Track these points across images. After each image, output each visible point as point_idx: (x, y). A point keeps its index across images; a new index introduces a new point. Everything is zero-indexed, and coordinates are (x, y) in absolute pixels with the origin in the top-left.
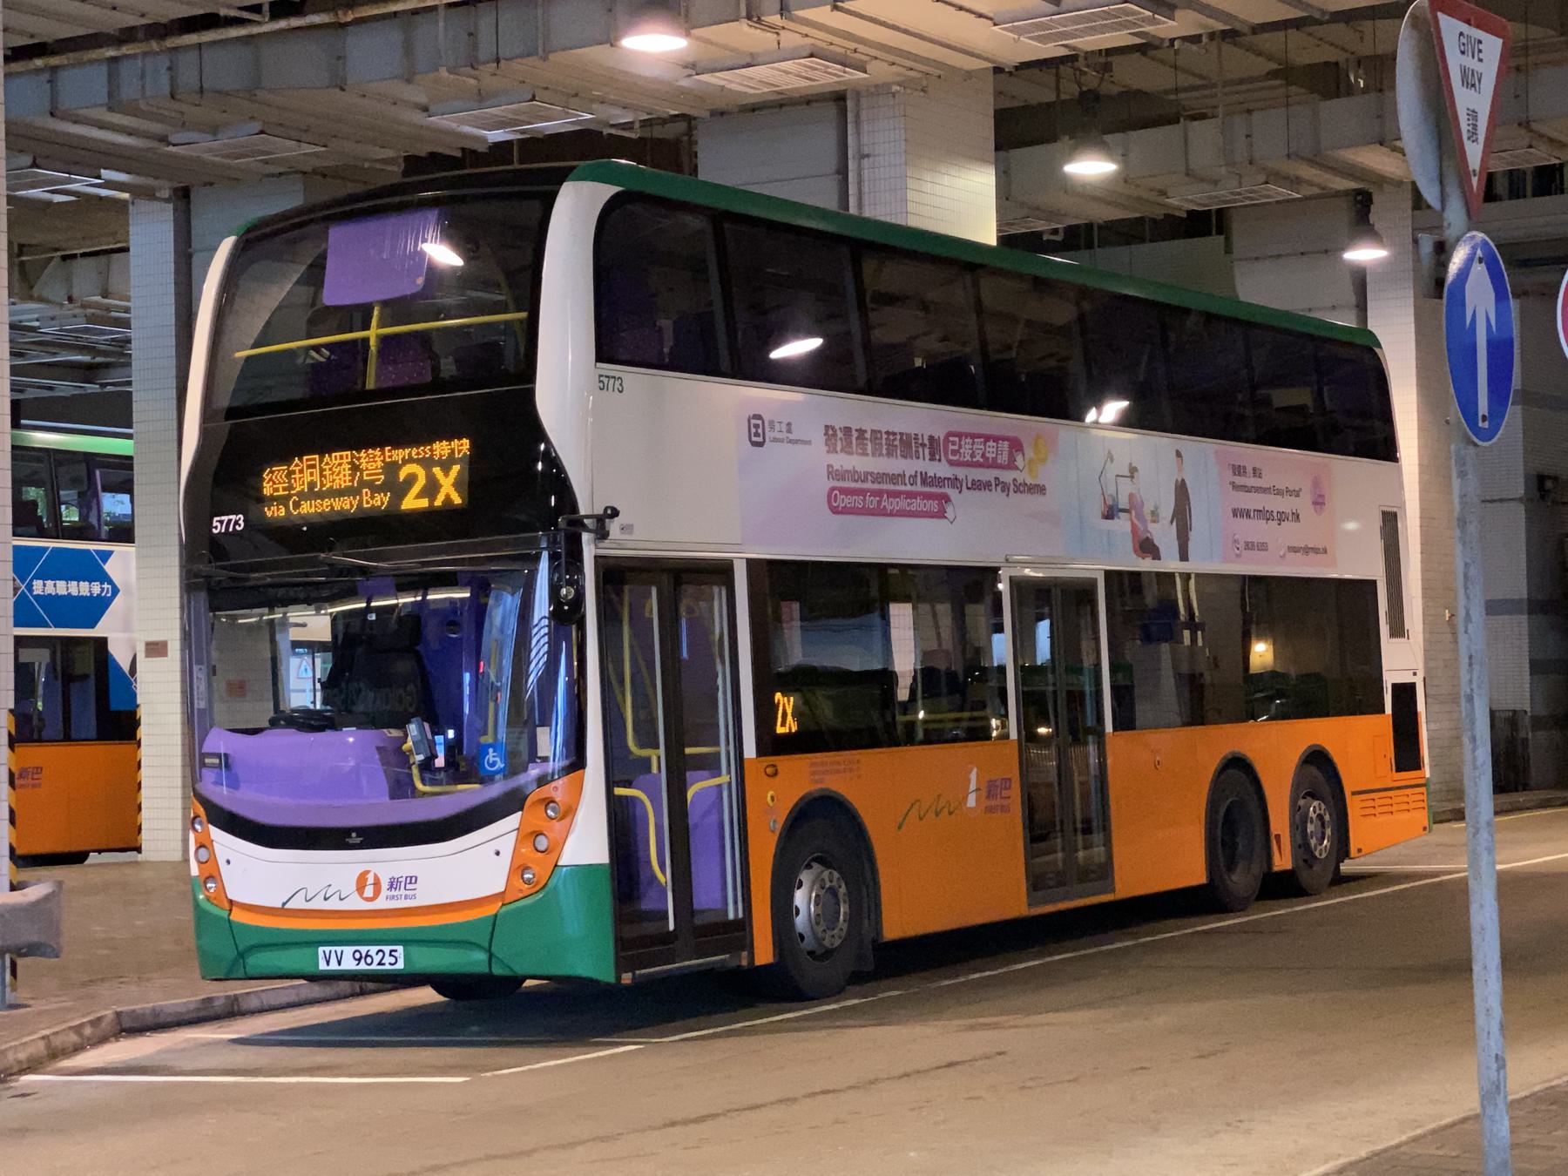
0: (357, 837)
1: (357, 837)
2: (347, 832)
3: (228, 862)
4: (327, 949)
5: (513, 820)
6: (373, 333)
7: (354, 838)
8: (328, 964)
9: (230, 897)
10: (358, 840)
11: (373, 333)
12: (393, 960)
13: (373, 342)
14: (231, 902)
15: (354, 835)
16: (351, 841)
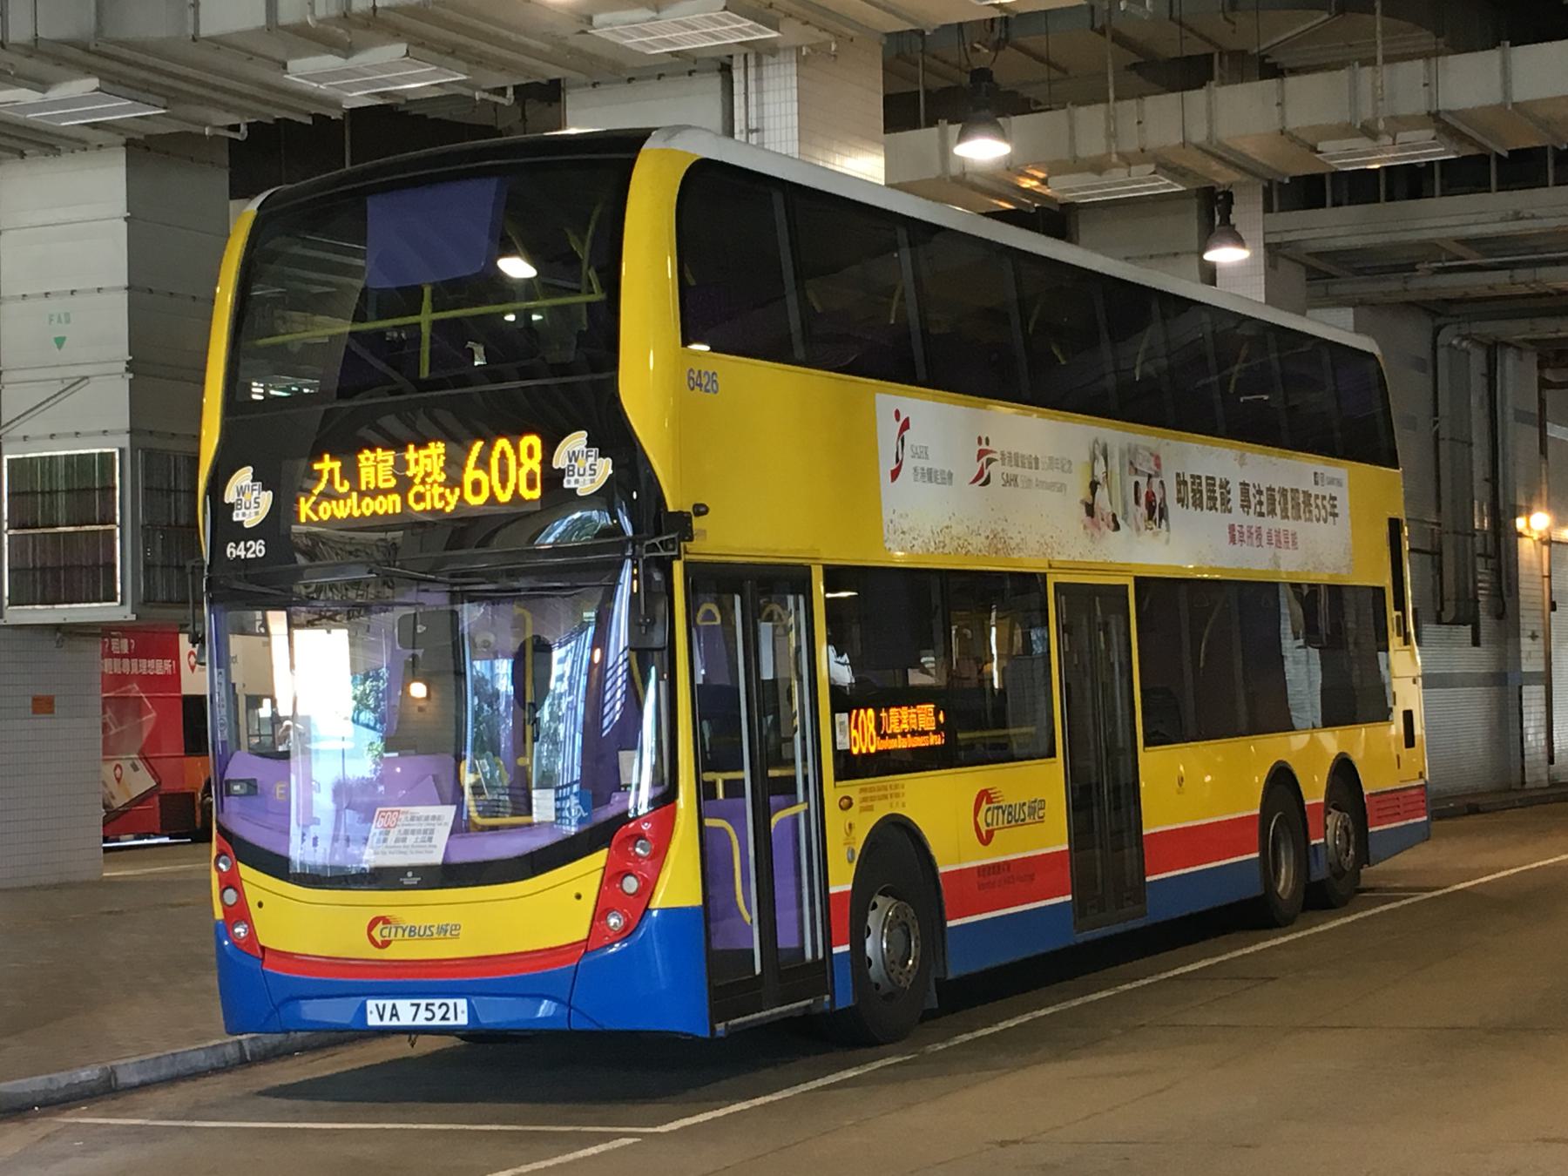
0: (413, 876)
1: (413, 876)
2: (402, 871)
3: (260, 905)
4: (381, 1003)
5: (600, 858)
6: (426, 318)
7: (410, 879)
8: (381, 1017)
9: (262, 944)
10: (415, 881)
11: (426, 318)
12: (429, 1015)
13: (426, 330)
14: (263, 949)
15: (410, 874)
16: (406, 882)
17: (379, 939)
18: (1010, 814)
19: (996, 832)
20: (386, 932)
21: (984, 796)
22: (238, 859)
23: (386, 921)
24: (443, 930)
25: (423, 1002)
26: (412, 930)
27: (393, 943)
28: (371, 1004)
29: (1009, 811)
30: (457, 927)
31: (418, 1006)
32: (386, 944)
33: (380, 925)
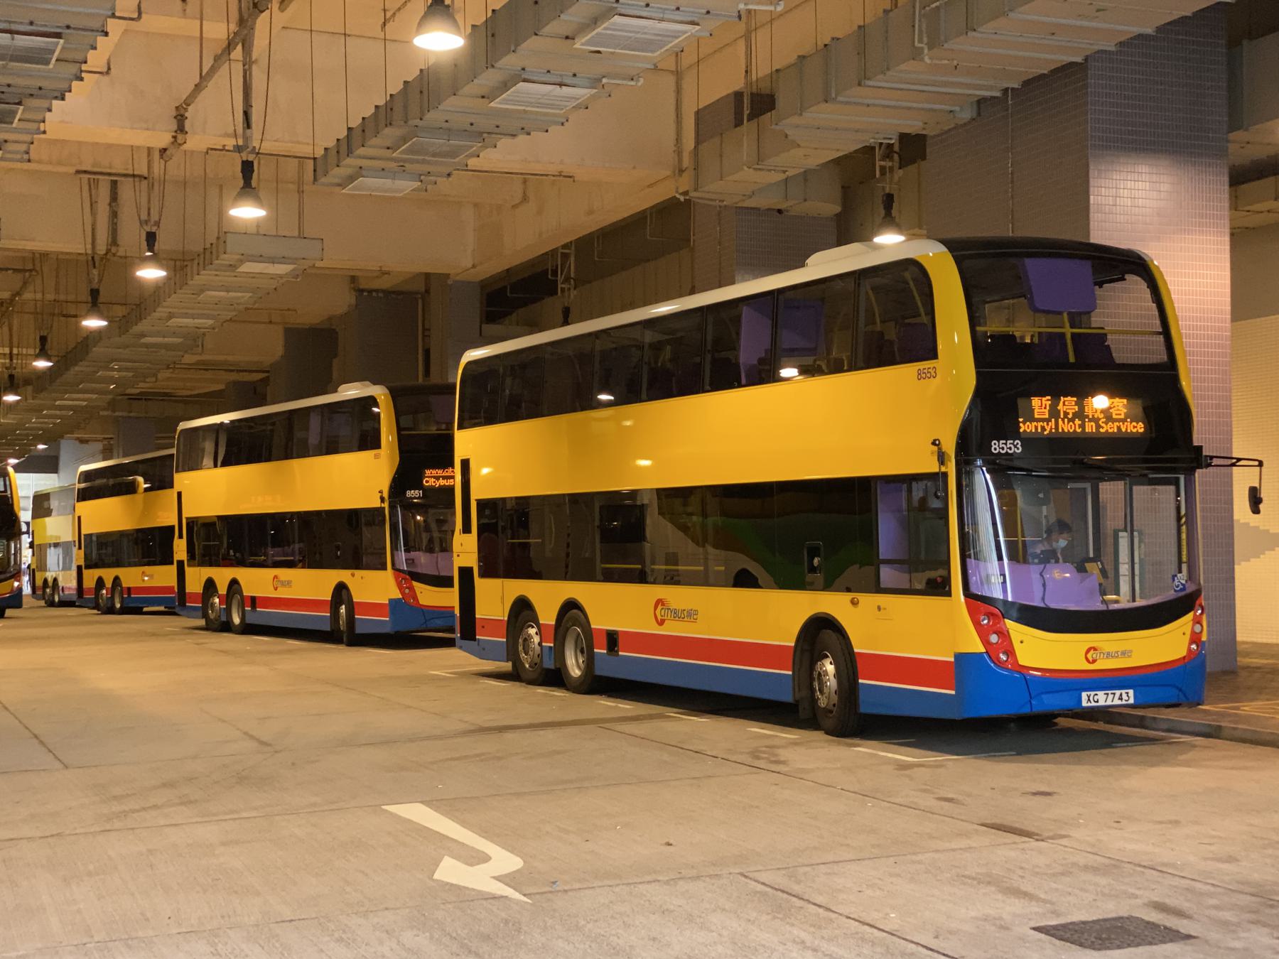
4: (1089, 693)
17: (1091, 659)
18: (675, 613)
19: (666, 622)
20: (1094, 656)
21: (659, 602)
22: (1004, 618)
23: (1095, 649)
24: (1124, 653)
25: (1110, 692)
26: (1108, 653)
27: (1098, 661)
28: (1084, 695)
29: (675, 612)
30: (1131, 651)
31: (1107, 694)
32: (1094, 661)
33: (1092, 652)
